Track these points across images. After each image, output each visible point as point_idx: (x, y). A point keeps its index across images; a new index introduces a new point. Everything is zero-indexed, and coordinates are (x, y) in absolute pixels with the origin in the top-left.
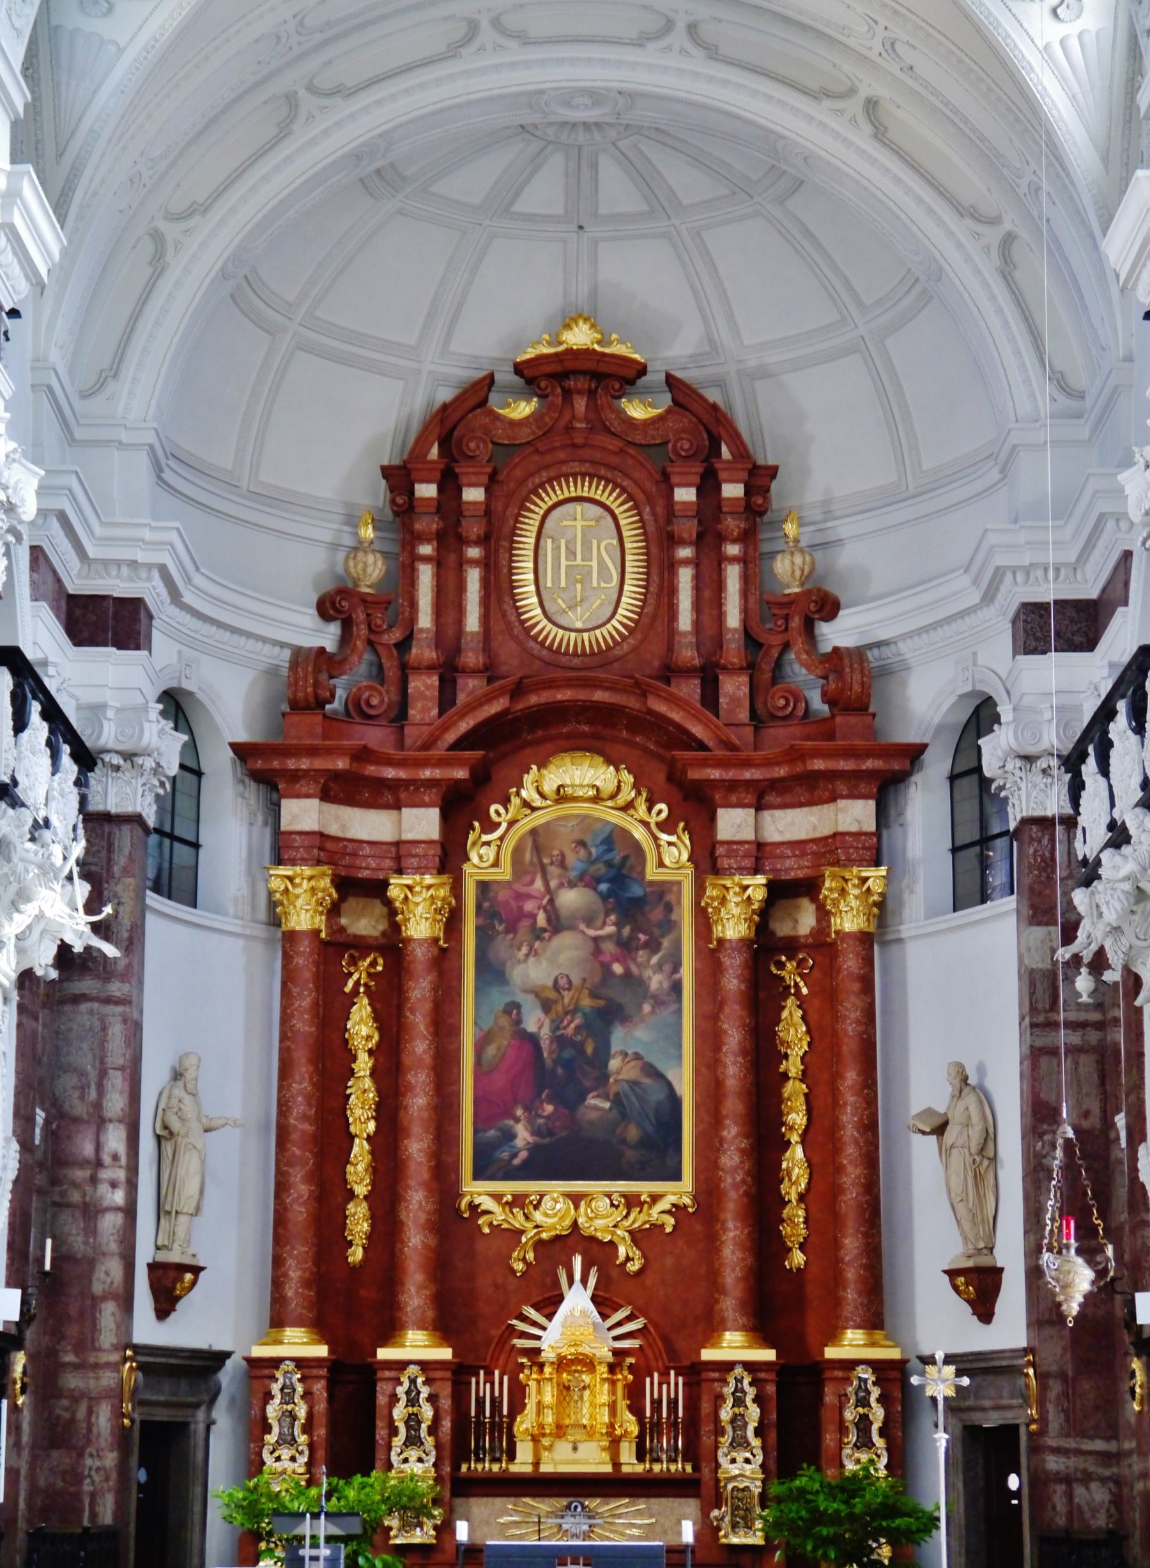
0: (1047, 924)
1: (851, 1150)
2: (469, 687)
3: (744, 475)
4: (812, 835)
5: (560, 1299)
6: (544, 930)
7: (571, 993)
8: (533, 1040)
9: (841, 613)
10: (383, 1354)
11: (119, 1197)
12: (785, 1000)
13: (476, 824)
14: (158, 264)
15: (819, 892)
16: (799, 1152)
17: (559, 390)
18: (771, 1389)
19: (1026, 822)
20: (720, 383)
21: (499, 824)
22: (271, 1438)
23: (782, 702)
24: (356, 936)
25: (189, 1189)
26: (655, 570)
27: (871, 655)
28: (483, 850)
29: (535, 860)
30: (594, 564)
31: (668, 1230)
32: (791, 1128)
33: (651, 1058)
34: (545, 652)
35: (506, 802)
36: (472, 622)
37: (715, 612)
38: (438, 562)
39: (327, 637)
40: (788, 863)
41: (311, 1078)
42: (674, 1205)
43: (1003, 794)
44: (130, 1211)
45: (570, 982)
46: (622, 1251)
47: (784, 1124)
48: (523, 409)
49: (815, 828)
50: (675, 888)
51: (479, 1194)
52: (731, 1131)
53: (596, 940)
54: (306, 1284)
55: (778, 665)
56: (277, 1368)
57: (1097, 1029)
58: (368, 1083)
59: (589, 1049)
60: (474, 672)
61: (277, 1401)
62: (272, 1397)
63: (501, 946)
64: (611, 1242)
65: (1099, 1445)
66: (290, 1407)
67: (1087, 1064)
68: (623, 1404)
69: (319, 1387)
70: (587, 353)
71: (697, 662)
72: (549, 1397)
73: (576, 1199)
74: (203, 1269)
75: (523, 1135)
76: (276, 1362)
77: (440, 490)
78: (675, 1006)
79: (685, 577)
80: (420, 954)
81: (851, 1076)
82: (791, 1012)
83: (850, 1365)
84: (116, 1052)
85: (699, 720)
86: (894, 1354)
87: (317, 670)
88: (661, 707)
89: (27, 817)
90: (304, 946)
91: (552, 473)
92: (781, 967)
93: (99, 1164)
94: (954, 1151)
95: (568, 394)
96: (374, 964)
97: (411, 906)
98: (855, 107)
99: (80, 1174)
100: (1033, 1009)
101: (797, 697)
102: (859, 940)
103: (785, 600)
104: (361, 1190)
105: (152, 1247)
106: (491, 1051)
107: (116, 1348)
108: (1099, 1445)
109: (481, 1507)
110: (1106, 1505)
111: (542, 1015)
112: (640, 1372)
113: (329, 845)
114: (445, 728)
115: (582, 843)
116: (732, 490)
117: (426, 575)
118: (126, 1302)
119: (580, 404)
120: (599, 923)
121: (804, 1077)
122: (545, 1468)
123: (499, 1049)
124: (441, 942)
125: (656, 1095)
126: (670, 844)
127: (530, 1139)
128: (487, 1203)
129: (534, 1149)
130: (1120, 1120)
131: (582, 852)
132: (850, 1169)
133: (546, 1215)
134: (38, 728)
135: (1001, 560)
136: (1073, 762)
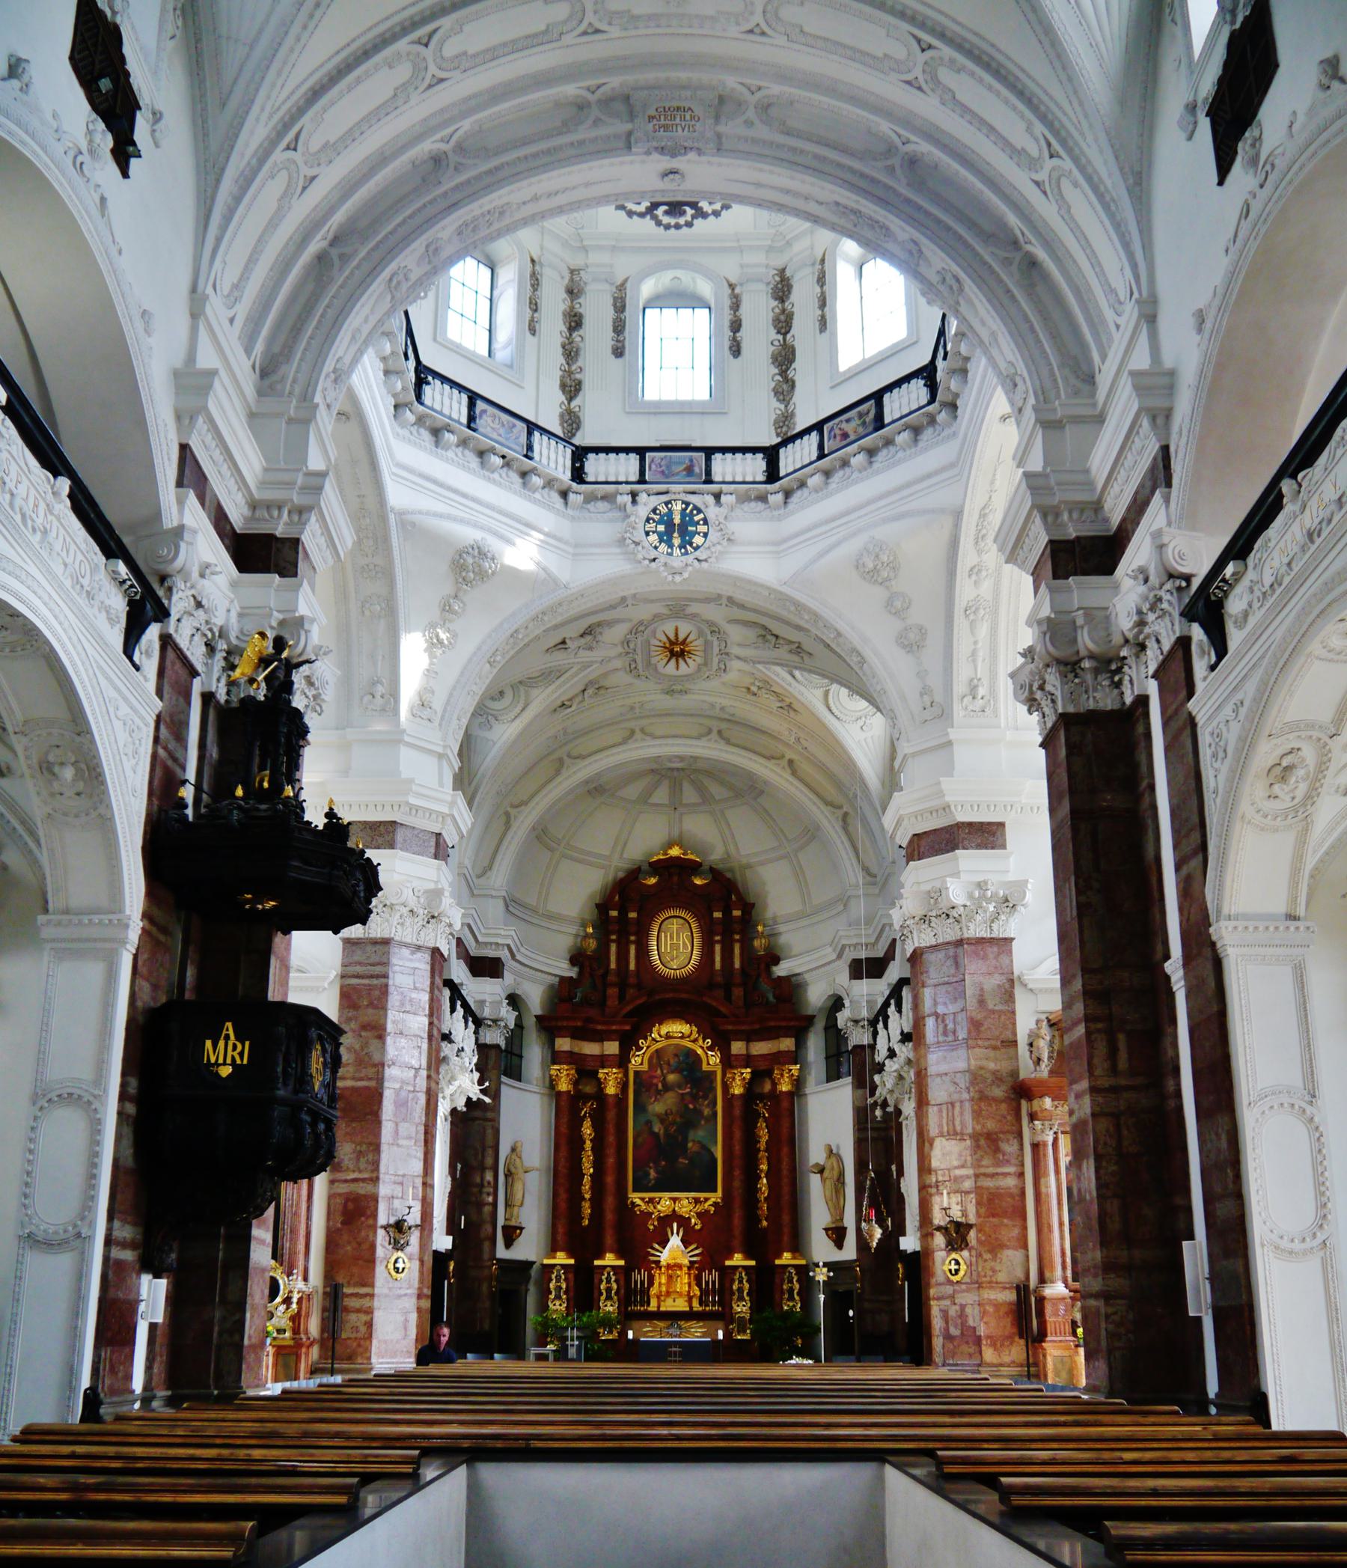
5: (668, 1241)
8: (656, 1135)
10: (597, 1263)
11: (490, 1199)
14: (508, 825)
16: (765, 1181)
18: (754, 1277)
19: (855, 1047)
20: (731, 870)
25: (518, 1196)
27: (793, 979)
35: (645, 1039)
36: (632, 966)
38: (618, 942)
39: (572, 973)
44: (495, 1204)
48: (653, 881)
52: (737, 1173)
68: (693, 1283)
69: (571, 1276)
70: (678, 858)
72: (663, 1281)
73: (674, 1200)
75: (653, 1174)
76: (553, 1266)
79: (718, 948)
80: (611, 1100)
81: (785, 1150)
82: (762, 1124)
83: (786, 1266)
84: (489, 1141)
86: (803, 1262)
88: (709, 1001)
89: (455, 1047)
90: (564, 1098)
93: (482, 1186)
98: (785, 762)
99: (475, 1190)
104: (587, 1196)
106: (640, 1140)
109: (636, 1324)
112: (701, 1270)
115: (676, 1055)
116: (737, 913)
117: (613, 947)
119: (675, 879)
121: (766, 1150)
122: (662, 1309)
128: (638, 1202)
129: (656, 1179)
130: (894, 1168)
134: (460, 1011)
135: (844, 942)
136: (873, 1023)
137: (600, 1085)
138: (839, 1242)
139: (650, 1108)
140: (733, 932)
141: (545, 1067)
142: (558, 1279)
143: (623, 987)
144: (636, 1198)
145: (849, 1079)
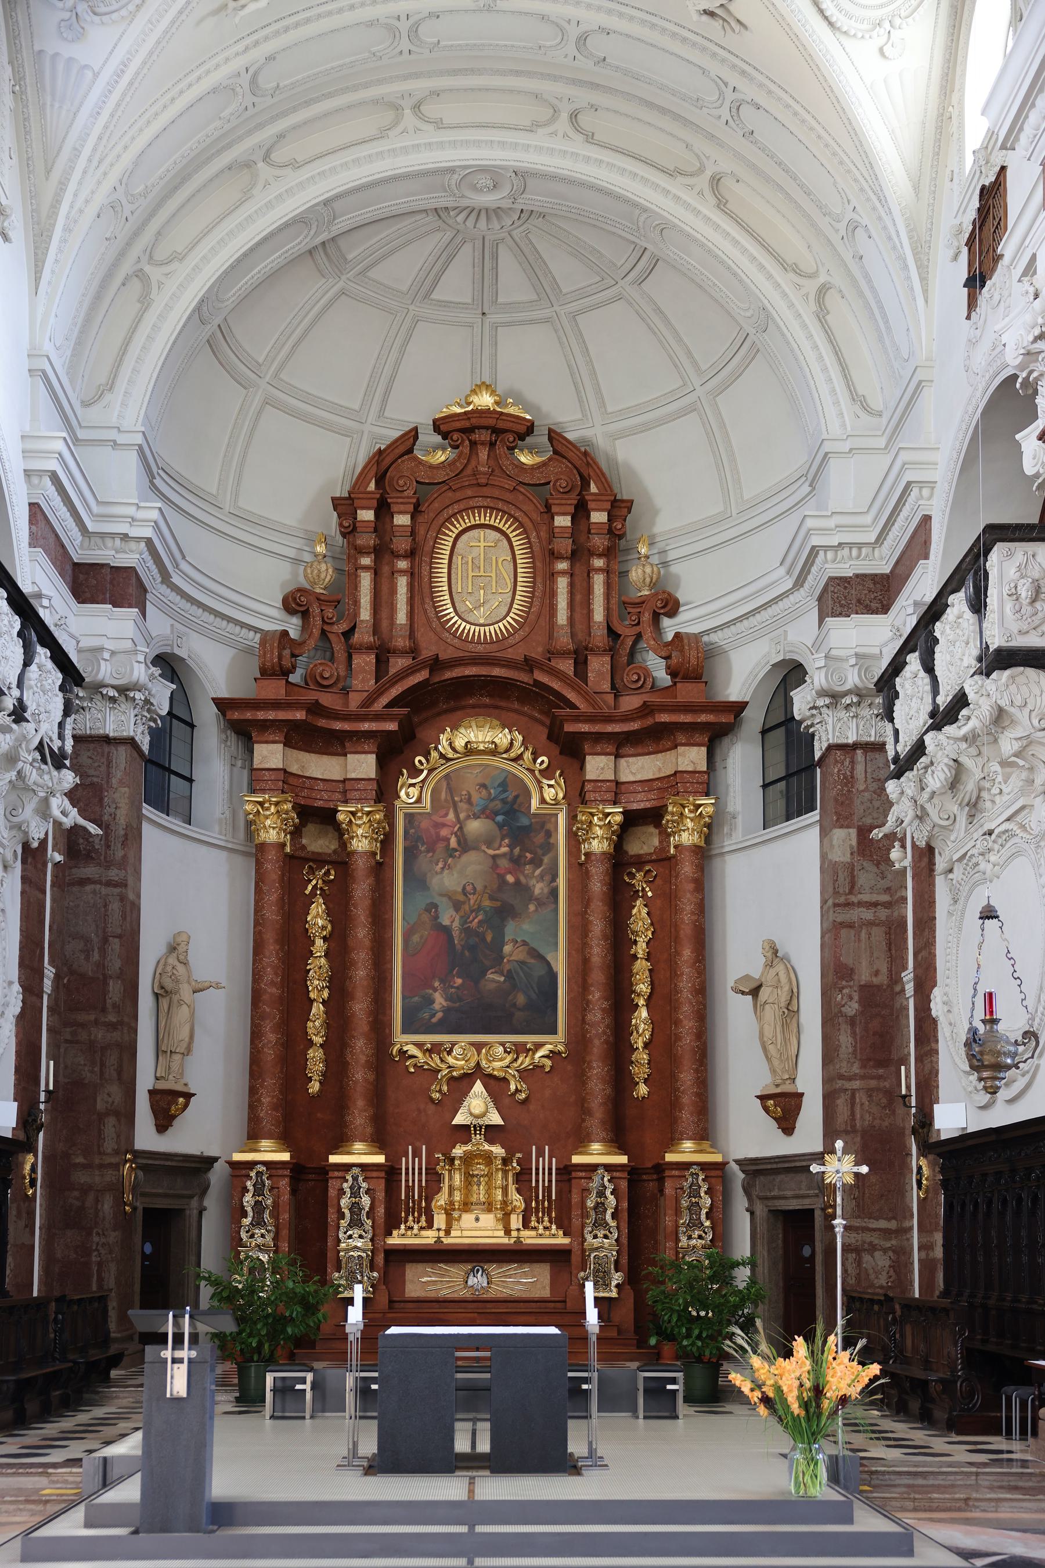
0: (848, 827)
1: (686, 1008)
2: (398, 664)
3: (608, 506)
4: (657, 776)
6: (455, 850)
7: (475, 897)
8: (447, 930)
9: (681, 609)
12: (635, 901)
13: (405, 771)
15: (662, 817)
16: (644, 1013)
17: (467, 442)
21: (422, 771)
22: (247, 1221)
23: (635, 677)
24: (313, 853)
26: (539, 580)
28: (411, 789)
29: (449, 798)
30: (493, 575)
31: (547, 1070)
32: (639, 995)
33: (534, 945)
34: (456, 641)
35: (427, 755)
36: (401, 617)
37: (585, 612)
39: (293, 626)
40: (639, 797)
41: (277, 954)
42: (551, 1051)
43: (811, 730)
45: (474, 888)
46: (513, 1087)
47: (634, 992)
49: (660, 769)
50: (553, 820)
51: (407, 1044)
52: (596, 996)
53: (494, 857)
54: (275, 1107)
55: (632, 654)
56: (251, 1169)
57: (886, 908)
58: (323, 961)
59: (489, 938)
60: (403, 653)
61: (250, 1194)
62: (248, 1191)
63: (423, 861)
64: (505, 1080)
65: (883, 1224)
66: (260, 1199)
67: (878, 933)
71: (571, 647)
74: (194, 1095)
75: (439, 1001)
77: (377, 515)
78: (553, 906)
79: (562, 584)
80: (361, 865)
81: (687, 953)
85: (573, 688)
87: (281, 647)
88: (544, 679)
90: (272, 855)
91: (462, 507)
92: (632, 876)
94: (767, 1007)
95: (473, 444)
96: (327, 873)
97: (355, 828)
100: (836, 893)
101: (647, 673)
102: (693, 851)
103: (637, 601)
104: (318, 1040)
105: (152, 1079)
106: (416, 938)
107: (117, 1152)
108: (883, 1224)
110: (886, 1269)
111: (454, 913)
113: (291, 780)
114: (378, 693)
115: (484, 786)
118: (128, 1116)
120: (496, 845)
123: (421, 937)
124: (378, 857)
125: (539, 971)
126: (550, 786)
127: (445, 1004)
128: (413, 1050)
129: (447, 1011)
130: (908, 976)
131: (484, 792)
132: (685, 1022)
133: (457, 1059)
137: (340, 833)
138: (787, 1124)
139: (435, 882)
140: (591, 553)
141: (234, 801)
142: (258, 1191)
143: (383, 654)
144: (405, 1042)
145: (814, 816)
